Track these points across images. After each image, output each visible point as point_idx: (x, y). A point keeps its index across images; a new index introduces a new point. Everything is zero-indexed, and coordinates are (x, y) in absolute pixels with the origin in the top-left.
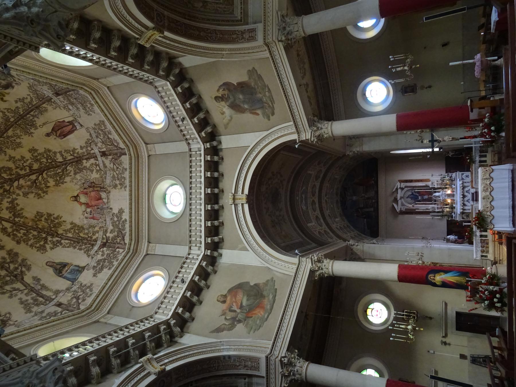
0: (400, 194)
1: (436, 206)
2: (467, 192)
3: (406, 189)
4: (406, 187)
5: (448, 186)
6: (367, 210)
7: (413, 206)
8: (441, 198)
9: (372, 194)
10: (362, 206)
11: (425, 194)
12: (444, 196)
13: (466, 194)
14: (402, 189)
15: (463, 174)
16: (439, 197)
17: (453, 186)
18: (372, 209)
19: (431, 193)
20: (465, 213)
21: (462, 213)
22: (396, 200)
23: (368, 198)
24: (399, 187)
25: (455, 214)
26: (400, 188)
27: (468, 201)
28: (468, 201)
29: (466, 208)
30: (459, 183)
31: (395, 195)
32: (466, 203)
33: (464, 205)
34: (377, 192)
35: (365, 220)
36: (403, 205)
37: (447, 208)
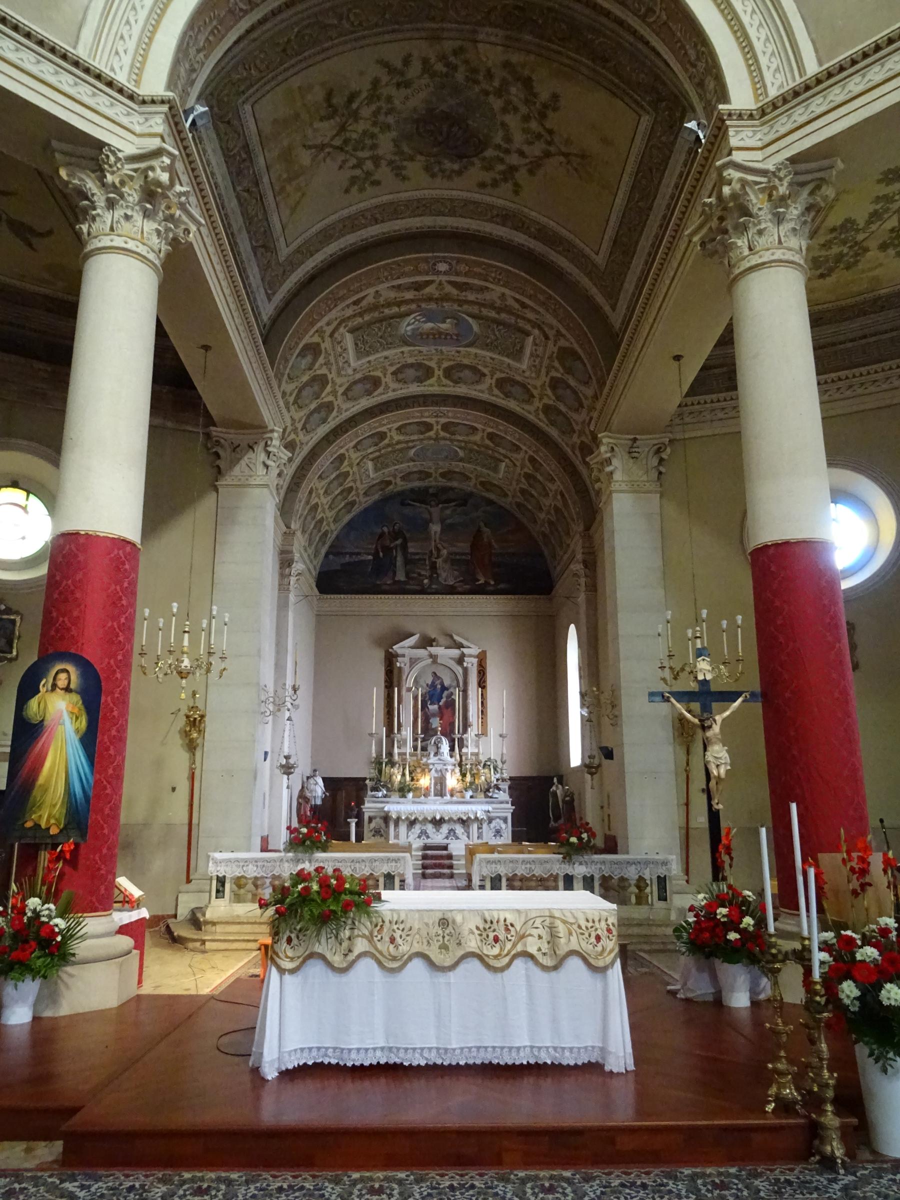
0: (445, 654)
1: (409, 749)
2: (452, 831)
3: (459, 670)
4: (466, 671)
8: (433, 759)
9: (447, 576)
11: (442, 715)
13: (445, 829)
14: (460, 661)
19: (448, 732)
22: (427, 642)
23: (433, 567)
26: (463, 655)
27: (424, 833)
28: (424, 833)
29: (403, 828)
31: (442, 640)
32: (417, 829)
33: (412, 823)
34: (451, 591)
36: (413, 662)
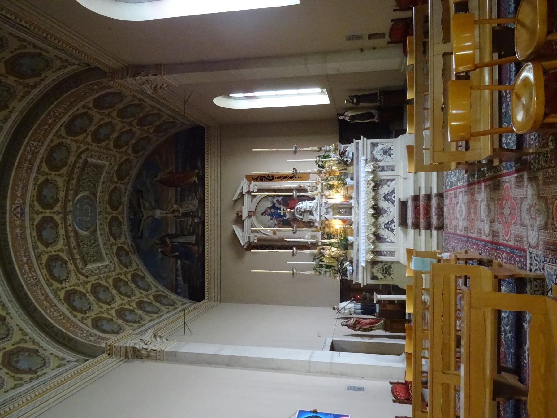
0: (247, 207)
2: (386, 197)
5: (335, 182)
6: (182, 240)
7: (274, 233)
9: (192, 205)
10: (172, 230)
12: (323, 211)
13: (384, 204)
15: (374, 145)
16: (311, 213)
17: (348, 180)
18: (193, 239)
20: (378, 262)
21: (374, 263)
22: (239, 221)
23: (186, 215)
24: (245, 191)
25: (351, 262)
26: (249, 192)
27: (388, 226)
28: (388, 226)
29: (383, 247)
30: (364, 171)
31: (237, 209)
32: (384, 233)
33: (378, 238)
34: (202, 202)
35: (179, 261)
37: (331, 245)
